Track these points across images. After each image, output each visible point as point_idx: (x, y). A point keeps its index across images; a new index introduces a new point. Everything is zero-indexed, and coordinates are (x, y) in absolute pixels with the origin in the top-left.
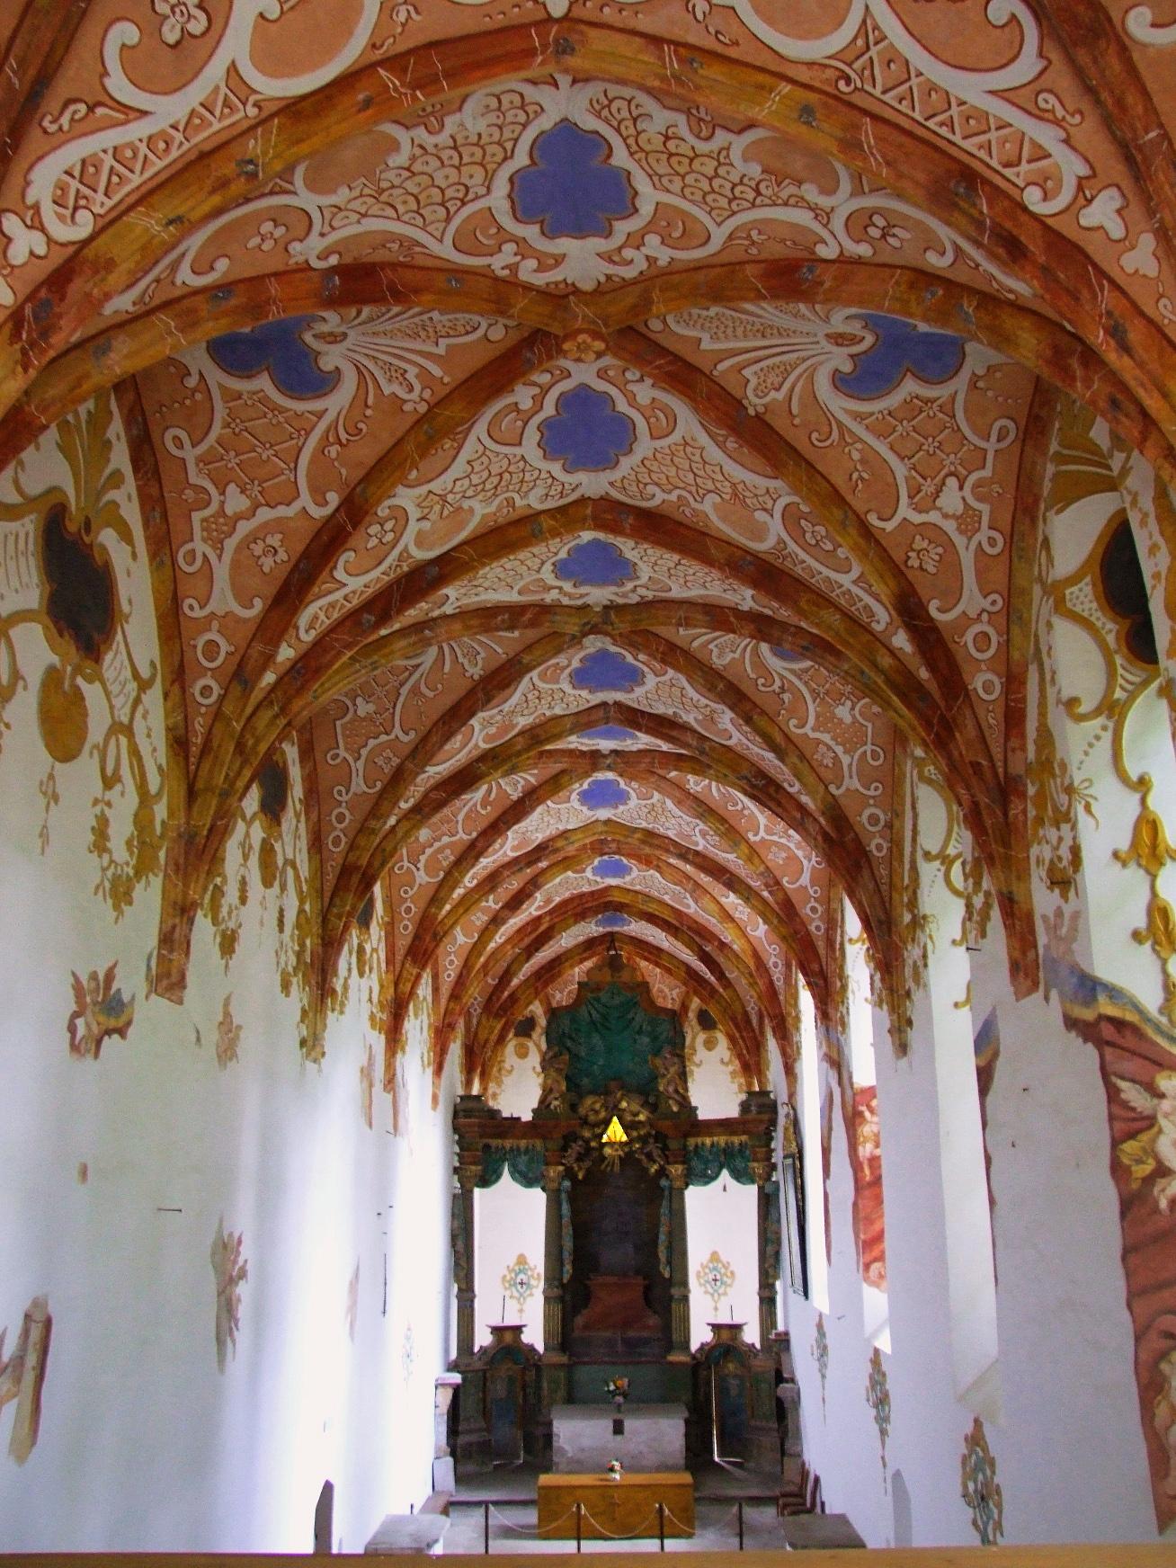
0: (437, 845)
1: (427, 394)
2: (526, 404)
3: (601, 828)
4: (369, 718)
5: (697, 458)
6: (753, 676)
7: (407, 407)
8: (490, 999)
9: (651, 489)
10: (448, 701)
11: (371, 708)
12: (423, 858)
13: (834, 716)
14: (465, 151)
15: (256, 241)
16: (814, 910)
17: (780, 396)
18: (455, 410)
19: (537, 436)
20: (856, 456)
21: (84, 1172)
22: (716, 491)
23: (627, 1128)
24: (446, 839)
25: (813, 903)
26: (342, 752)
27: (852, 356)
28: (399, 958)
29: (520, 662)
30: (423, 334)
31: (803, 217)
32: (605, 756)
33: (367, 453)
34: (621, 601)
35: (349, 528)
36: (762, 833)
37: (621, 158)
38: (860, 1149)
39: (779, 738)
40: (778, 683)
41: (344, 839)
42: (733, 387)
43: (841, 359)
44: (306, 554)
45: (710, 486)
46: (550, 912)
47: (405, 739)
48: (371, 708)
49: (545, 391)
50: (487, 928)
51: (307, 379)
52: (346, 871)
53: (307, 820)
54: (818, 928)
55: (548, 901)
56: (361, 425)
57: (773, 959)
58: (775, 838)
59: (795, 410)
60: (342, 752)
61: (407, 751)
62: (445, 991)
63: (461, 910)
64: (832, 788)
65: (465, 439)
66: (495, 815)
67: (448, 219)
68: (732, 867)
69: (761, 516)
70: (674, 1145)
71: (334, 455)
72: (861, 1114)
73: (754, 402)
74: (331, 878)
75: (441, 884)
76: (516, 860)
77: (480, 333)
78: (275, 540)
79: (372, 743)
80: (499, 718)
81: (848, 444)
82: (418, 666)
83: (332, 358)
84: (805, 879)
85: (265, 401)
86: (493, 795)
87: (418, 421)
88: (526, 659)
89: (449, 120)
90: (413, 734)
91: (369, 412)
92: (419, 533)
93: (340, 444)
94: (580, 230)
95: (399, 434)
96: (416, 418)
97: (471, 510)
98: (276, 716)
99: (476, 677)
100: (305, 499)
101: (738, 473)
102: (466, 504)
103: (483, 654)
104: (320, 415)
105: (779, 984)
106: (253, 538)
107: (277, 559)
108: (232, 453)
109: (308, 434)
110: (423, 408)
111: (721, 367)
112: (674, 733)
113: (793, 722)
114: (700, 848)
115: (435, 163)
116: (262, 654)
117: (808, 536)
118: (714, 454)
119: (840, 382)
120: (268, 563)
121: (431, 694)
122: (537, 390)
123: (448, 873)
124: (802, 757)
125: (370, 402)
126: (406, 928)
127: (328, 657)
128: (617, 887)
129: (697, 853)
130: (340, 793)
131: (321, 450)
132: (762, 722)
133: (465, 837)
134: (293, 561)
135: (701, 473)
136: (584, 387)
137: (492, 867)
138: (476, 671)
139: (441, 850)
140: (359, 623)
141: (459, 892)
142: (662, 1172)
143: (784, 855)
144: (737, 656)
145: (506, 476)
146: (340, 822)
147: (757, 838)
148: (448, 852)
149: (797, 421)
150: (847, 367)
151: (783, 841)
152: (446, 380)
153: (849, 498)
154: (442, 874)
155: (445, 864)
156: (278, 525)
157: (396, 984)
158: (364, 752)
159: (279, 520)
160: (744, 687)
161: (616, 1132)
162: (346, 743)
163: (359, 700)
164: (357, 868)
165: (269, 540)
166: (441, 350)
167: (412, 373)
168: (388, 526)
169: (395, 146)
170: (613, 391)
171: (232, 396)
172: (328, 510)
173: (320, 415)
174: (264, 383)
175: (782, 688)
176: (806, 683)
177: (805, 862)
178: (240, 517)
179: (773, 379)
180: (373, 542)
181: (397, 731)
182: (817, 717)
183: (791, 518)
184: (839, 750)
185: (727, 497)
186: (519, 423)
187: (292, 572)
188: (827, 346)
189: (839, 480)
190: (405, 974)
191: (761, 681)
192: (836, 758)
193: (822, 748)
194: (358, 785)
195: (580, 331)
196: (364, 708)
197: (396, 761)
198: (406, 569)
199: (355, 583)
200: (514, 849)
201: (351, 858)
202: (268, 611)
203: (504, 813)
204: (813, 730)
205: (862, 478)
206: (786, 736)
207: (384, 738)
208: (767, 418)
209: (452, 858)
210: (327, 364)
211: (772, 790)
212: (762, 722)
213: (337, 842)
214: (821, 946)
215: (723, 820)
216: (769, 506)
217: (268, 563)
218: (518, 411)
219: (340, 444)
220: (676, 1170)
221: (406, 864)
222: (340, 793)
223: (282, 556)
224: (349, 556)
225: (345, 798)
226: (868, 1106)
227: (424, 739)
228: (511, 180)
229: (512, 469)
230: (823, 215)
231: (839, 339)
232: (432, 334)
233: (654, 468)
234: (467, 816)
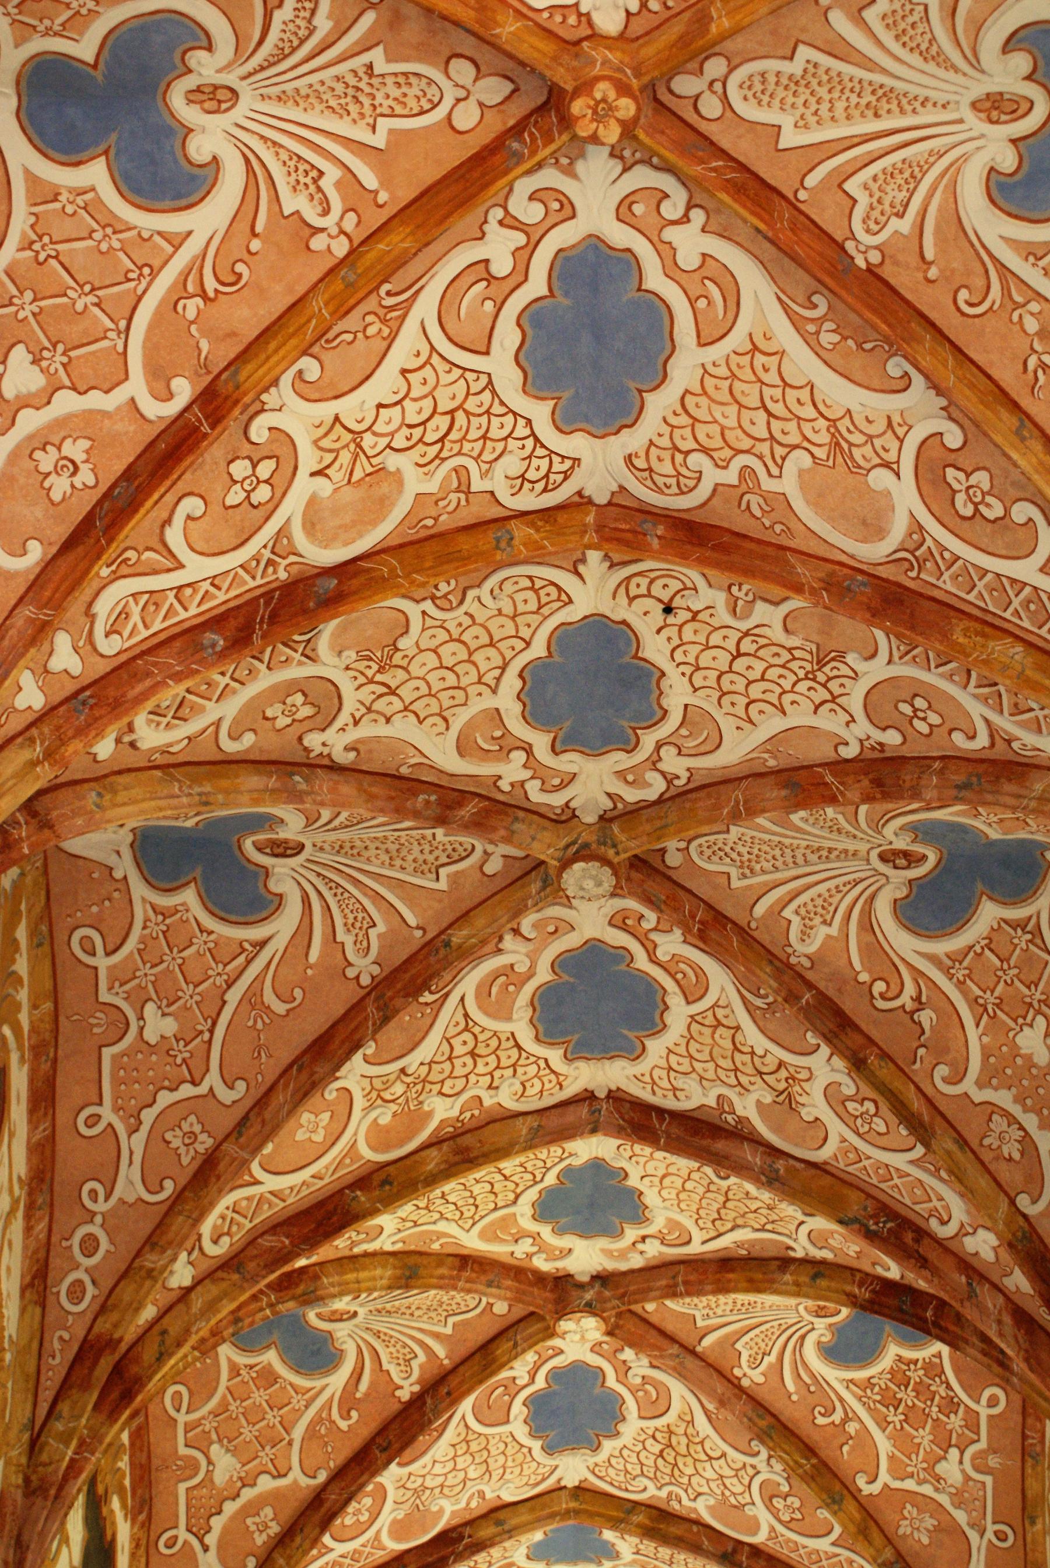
0: (248, 1494)
1: (350, 222)
2: (502, 266)
3: (565, 1503)
4: (164, 1047)
5: (772, 377)
6: (864, 977)
7: (318, 243)
9: (697, 460)
10: (313, 1026)
11: (169, 1026)
12: (217, 1523)
13: (1015, 1051)
17: (904, 226)
18: (398, 240)
19: (516, 337)
20: (1032, 325)
22: (805, 444)
24: (266, 1484)
26: (107, 1113)
27: (1014, 141)
29: (447, 944)
30: (353, 108)
32: (581, 1286)
33: (248, 317)
34: (632, 795)
35: (206, 428)
36: (884, 1477)
39: (916, 1104)
40: (910, 990)
41: (91, 1291)
42: (828, 219)
43: (995, 147)
44: (128, 474)
45: (794, 438)
47: (226, 1096)
48: (169, 1026)
51: (166, 178)
52: (89, 1350)
53: (28, 1229)
56: (240, 267)
58: (910, 1485)
59: (929, 255)
60: (107, 1113)
61: (229, 1121)
64: (1023, 1201)
65: (403, 318)
66: (365, 1433)
69: (881, 479)
71: (191, 314)
73: (865, 245)
74: (58, 1363)
77: (440, 113)
78: (76, 450)
79: (165, 1098)
80: (399, 1089)
81: (1018, 306)
82: (262, 944)
83: (209, 138)
85: (94, 207)
86: (364, 1386)
87: (331, 271)
88: (458, 937)
90: (241, 1086)
91: (255, 245)
92: (313, 502)
93: (204, 295)
95: (301, 289)
96: (330, 263)
97: (397, 477)
98: (34, 763)
99: (365, 980)
100: (136, 386)
101: (840, 394)
102: (393, 462)
103: (381, 928)
104: (177, 241)
106: (41, 441)
107: (76, 482)
108: (29, 295)
109: (154, 274)
110: (341, 248)
111: (811, 181)
112: (720, 1145)
113: (942, 1070)
114: (760, 1538)
116: (31, 621)
117: (960, 499)
118: (803, 362)
119: (1001, 190)
120: (59, 486)
121: (280, 1008)
122: (520, 239)
124: (962, 1142)
125: (259, 229)
127: (139, 688)
130: (93, 1194)
131: (173, 303)
132: (884, 1072)
133: (305, 1481)
134: (103, 488)
135: (778, 409)
136: (595, 243)
138: (365, 968)
139: (252, 1508)
140: (199, 648)
143: (930, 1523)
144: (834, 931)
145: (460, 416)
146: (79, 1282)
147: (875, 1488)
148: (268, 1512)
149: (933, 273)
150: (1008, 161)
151: (927, 1490)
152: (383, 197)
153: (1025, 402)
155: (260, 1539)
156: (85, 424)
158: (148, 1116)
159: (90, 416)
160: (847, 1006)
162: (115, 1098)
163: (150, 1009)
164: (112, 1344)
165: (68, 449)
166: (379, 140)
167: (332, 174)
168: (265, 469)
171: (44, 195)
172: (172, 409)
173: (177, 241)
174: (95, 174)
175: (918, 999)
176: (960, 984)
177: (973, 1535)
178: (25, 402)
179: (895, 195)
180: (235, 496)
181: (213, 1079)
182: (986, 1056)
183: (933, 468)
184: (1030, 1122)
185: (821, 453)
186: (489, 305)
187: (100, 503)
188: (975, 124)
189: (1007, 376)
191: (879, 987)
192: (1027, 1141)
193: (999, 1123)
194: (130, 1183)
195: (598, 79)
196: (158, 1025)
197: (205, 1143)
198: (283, 575)
199: (198, 568)
200: (398, 1530)
201: (103, 1326)
202: (48, 565)
203: (382, 1431)
204: (980, 1084)
205: (1043, 366)
206: (929, 1101)
207: (187, 1090)
208: (887, 272)
209: (275, 1529)
210: (200, 149)
211: (909, 1237)
212: (884, 1072)
213: (77, 1291)
215: (809, 1450)
216: (892, 457)
217: (59, 486)
218: (490, 279)
219: (204, 295)
221: (183, 1535)
222: (93, 1194)
223: (85, 476)
224: (192, 505)
225: (101, 1206)
227: (261, 1103)
229: (471, 405)
231: (996, 107)
232: (367, 110)
233: (702, 414)
234: (311, 1432)
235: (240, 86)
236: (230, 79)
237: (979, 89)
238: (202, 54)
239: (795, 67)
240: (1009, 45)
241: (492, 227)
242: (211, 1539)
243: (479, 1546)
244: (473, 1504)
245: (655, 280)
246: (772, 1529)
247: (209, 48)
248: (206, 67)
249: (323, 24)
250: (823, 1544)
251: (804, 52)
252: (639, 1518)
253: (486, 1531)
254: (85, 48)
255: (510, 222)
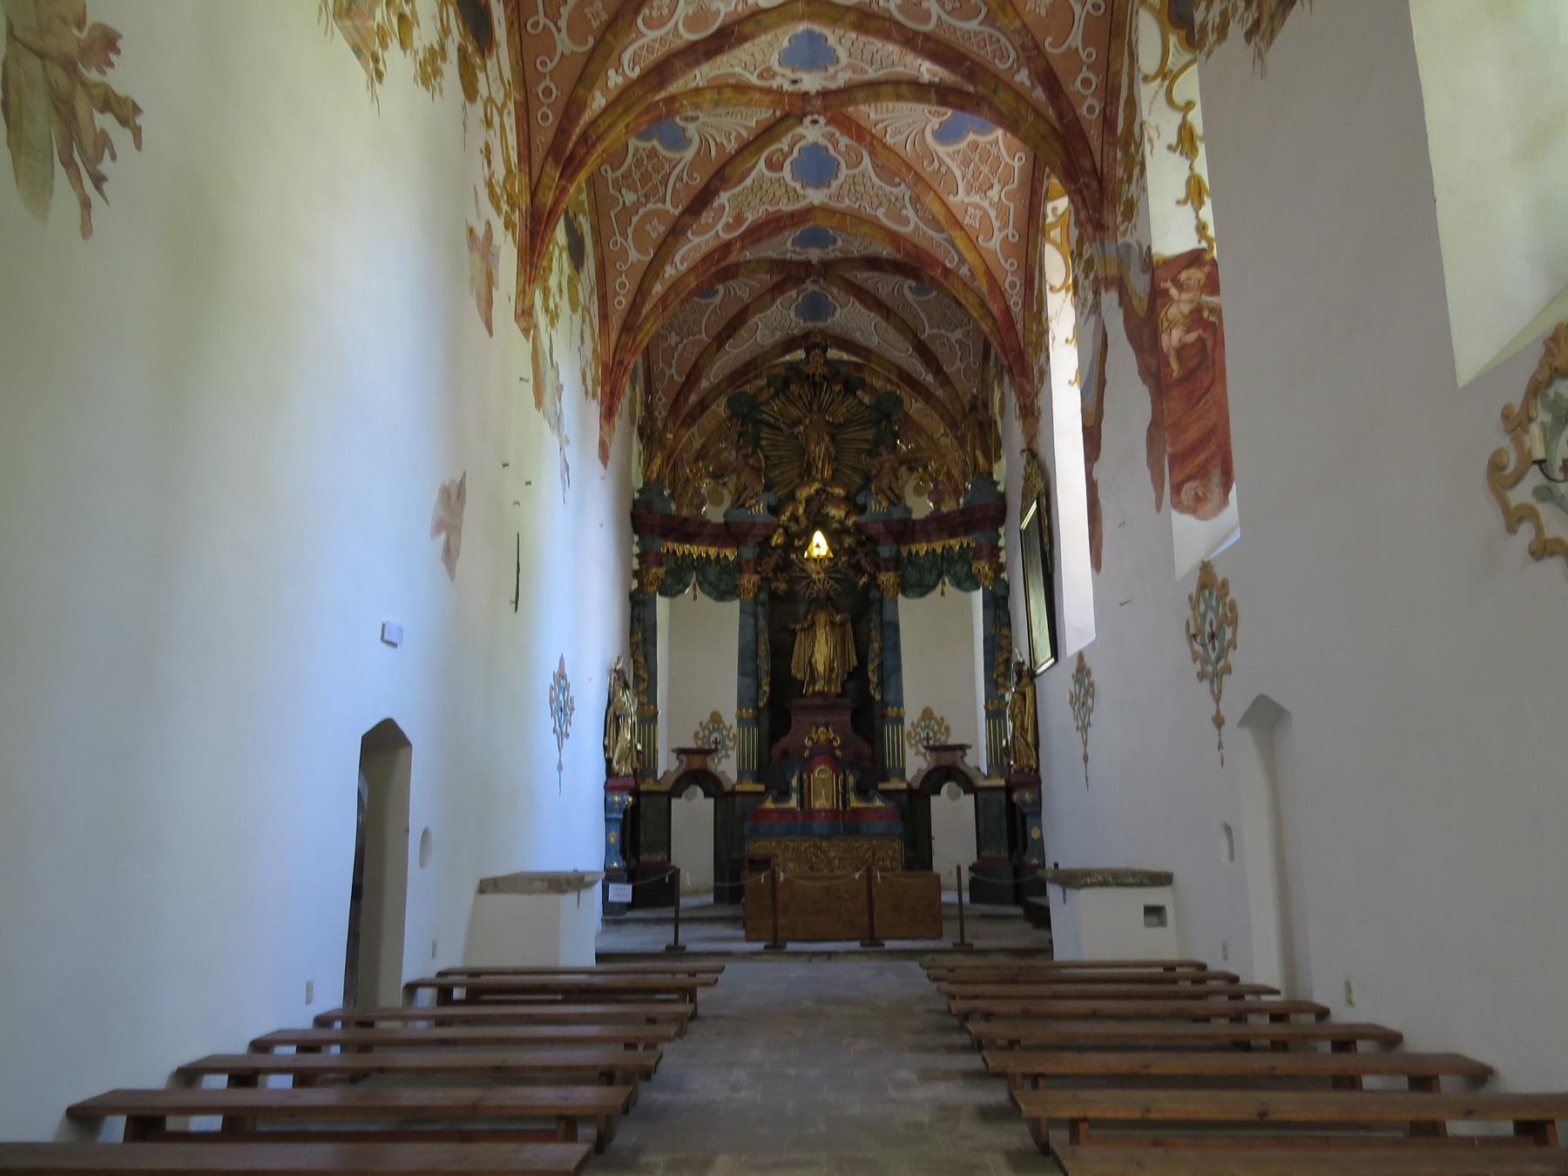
8: (676, 401)
16: (1086, 83)
23: (832, 537)
25: (1085, 73)
28: (537, 159)
38: (1165, 339)
46: (742, 237)
50: (664, 242)
54: (1091, 109)
55: (739, 219)
57: (1010, 278)
62: (616, 322)
63: (620, 109)
68: (972, 48)
70: (886, 551)
72: (1166, 292)
75: (591, 55)
76: (692, 46)
84: (1076, 38)
105: (1017, 310)
114: (930, 27)
123: (600, 41)
126: (545, 117)
128: (823, 208)
129: (927, 37)
137: (660, 51)
141: (615, 80)
142: (873, 583)
154: (591, 41)
155: (595, 24)
157: (533, 195)
161: (819, 545)
190: (545, 180)
209: (604, 16)
214: (1094, 136)
220: (887, 578)
221: (542, 20)
226: (1175, 281)
242: (563, 23)
243: (744, 39)
244: (740, 8)
246: (939, 18)
250: (973, 25)
252: (851, 17)
253: (748, 28)
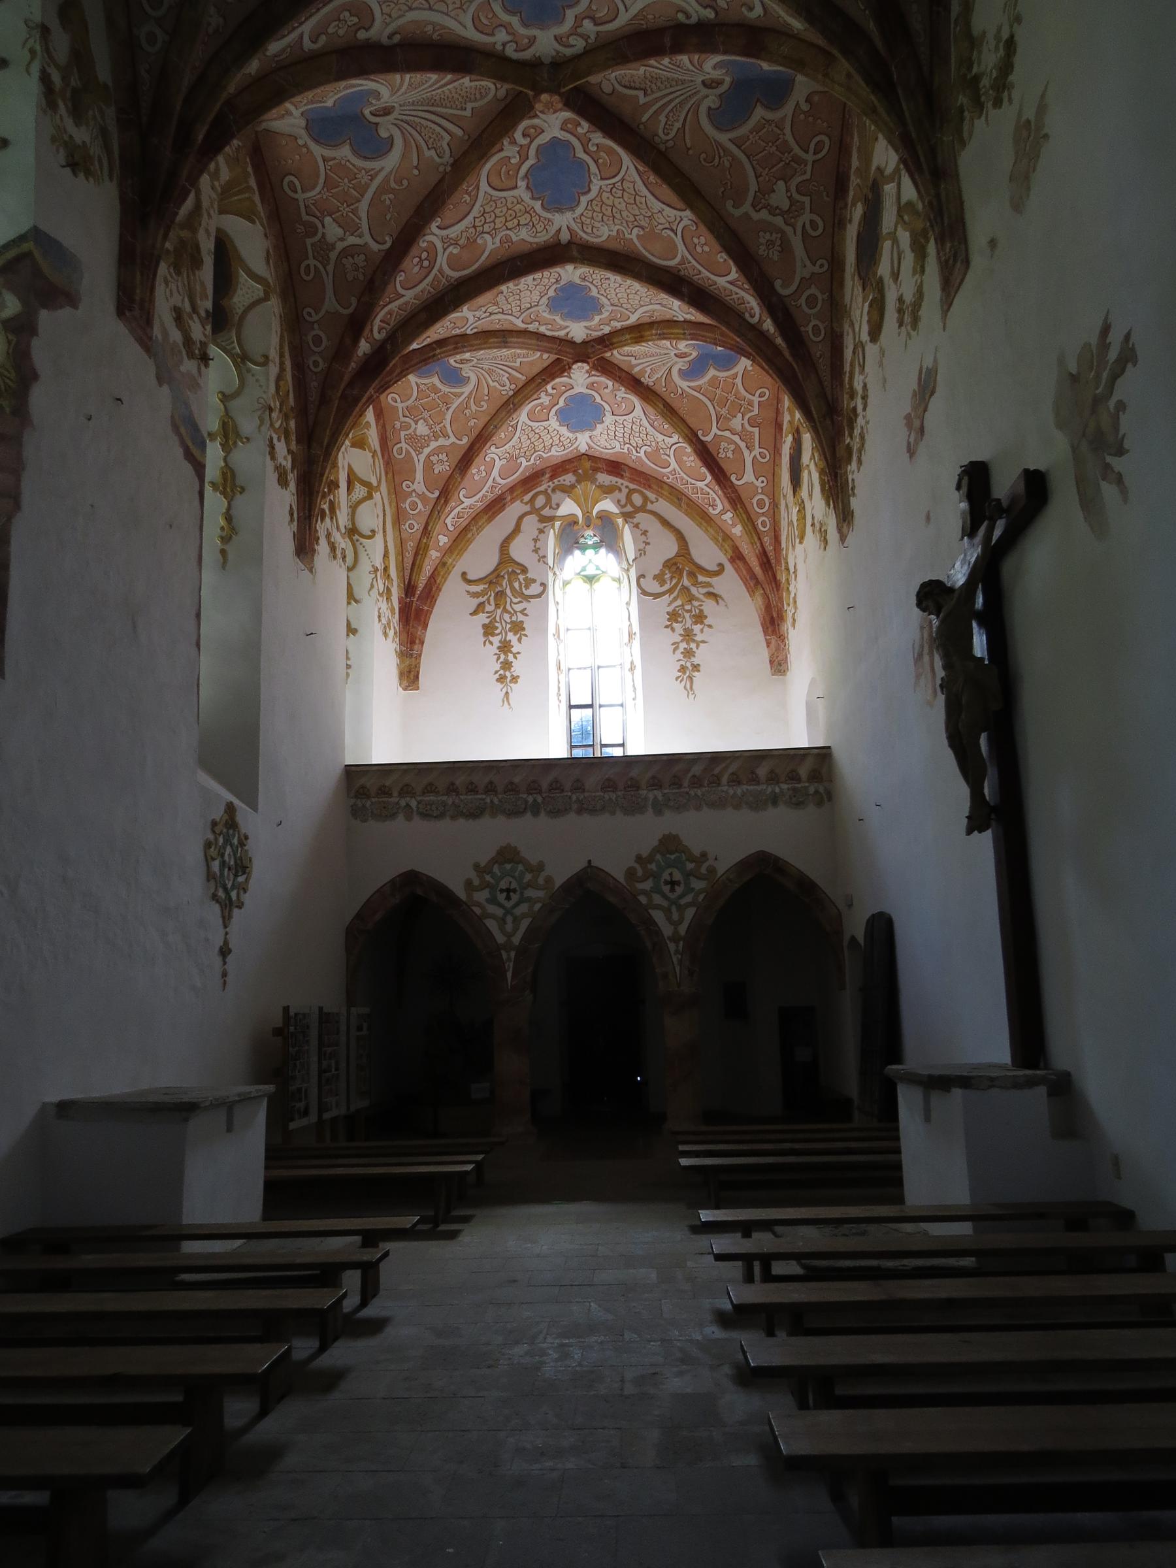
14: (609, 213)
15: (706, 249)
21: (928, 518)
31: (453, 232)
37: (537, 205)
49: (574, 32)
67: (623, 180)
89: (614, 233)
94: (560, 210)
115: (625, 214)
122: (579, 30)
169: (638, 236)
170: (522, 31)
228: (590, 190)
230: (448, 242)
231: (387, 111)
235: (701, 87)
236: (705, 91)
237: (395, 115)
238: (713, 106)
239: (469, 106)
240: (391, 139)
241: (593, 37)
245: (515, 20)
247: (710, 108)
248: (711, 100)
249: (662, 118)
251: (468, 113)
254: (759, 113)
255: (585, 37)
